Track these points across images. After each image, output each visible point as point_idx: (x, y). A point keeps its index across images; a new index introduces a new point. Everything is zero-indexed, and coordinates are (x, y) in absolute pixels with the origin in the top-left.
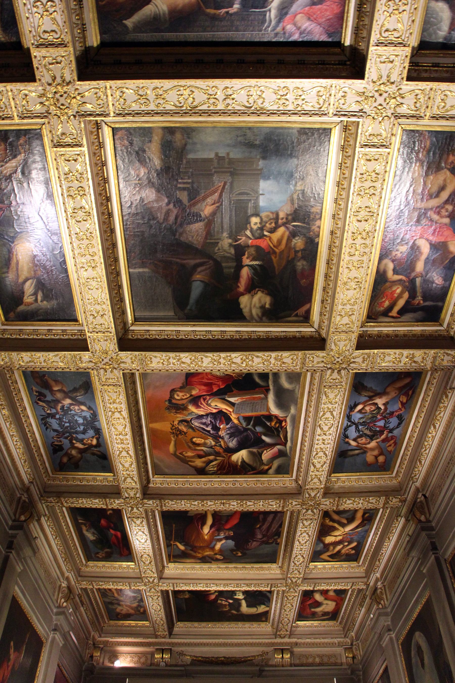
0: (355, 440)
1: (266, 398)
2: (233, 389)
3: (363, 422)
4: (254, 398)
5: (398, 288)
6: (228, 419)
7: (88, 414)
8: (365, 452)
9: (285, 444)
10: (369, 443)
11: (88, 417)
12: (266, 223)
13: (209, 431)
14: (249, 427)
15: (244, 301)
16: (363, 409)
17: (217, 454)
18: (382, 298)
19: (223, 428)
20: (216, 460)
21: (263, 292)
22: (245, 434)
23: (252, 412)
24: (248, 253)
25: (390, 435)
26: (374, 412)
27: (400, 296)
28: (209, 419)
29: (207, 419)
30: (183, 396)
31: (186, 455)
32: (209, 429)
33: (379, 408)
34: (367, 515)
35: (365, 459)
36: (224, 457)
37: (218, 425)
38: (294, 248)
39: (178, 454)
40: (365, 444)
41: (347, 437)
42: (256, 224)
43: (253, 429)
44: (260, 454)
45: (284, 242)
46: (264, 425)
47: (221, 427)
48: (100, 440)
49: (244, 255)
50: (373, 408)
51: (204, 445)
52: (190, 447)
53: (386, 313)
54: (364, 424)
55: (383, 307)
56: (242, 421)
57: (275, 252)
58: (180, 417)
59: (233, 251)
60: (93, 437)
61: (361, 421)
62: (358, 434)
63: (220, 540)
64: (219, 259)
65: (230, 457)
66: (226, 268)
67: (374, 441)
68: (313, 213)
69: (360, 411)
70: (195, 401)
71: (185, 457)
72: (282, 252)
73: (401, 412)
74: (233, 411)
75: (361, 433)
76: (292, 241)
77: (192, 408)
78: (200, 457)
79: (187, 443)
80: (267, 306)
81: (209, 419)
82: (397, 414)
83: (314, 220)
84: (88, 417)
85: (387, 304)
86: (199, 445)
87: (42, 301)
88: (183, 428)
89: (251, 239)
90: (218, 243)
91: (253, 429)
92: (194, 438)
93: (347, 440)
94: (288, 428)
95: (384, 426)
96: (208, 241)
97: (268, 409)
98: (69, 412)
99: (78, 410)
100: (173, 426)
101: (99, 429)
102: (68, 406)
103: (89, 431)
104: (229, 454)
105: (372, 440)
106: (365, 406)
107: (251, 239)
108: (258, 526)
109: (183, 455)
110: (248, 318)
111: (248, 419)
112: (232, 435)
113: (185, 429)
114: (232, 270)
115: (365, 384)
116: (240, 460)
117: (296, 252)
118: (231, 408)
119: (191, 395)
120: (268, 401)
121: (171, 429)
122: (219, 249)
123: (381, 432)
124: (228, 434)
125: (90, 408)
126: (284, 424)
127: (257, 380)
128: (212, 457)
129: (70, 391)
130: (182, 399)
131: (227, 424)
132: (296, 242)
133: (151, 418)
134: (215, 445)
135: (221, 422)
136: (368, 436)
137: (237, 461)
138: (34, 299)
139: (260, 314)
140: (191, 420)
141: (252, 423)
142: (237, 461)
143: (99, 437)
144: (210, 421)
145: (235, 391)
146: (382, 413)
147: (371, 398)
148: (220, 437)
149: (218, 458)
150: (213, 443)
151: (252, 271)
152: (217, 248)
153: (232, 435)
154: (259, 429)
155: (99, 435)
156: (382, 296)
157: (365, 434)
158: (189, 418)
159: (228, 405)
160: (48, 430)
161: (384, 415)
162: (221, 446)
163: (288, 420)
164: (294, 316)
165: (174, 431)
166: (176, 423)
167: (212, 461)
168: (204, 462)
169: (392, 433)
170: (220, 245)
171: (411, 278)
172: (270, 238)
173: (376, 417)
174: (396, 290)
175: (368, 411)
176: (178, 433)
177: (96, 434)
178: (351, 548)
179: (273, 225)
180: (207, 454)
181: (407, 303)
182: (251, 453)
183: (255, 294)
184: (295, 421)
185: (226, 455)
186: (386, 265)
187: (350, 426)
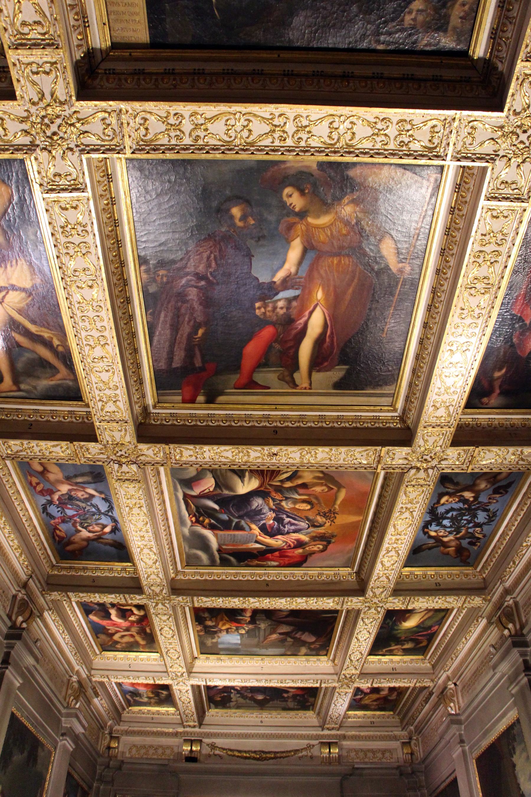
4: (233, 545)
6: (263, 529)
9: (185, 496)
10: (70, 490)
13: (288, 517)
14: (236, 520)
17: (279, 489)
19: (269, 520)
20: (282, 481)
22: (241, 513)
23: (234, 535)
31: (324, 488)
32: (287, 520)
36: (271, 485)
37: (276, 523)
39: (335, 488)
41: (103, 499)
43: (232, 518)
44: (217, 485)
46: (218, 520)
48: (436, 501)
51: (295, 501)
52: (317, 498)
56: (245, 526)
58: (321, 530)
63: (286, 283)
65: (261, 486)
70: (300, 544)
71: (326, 485)
74: (257, 536)
77: (304, 538)
78: (304, 486)
79: (319, 503)
81: (286, 529)
86: (304, 501)
88: (320, 519)
91: (232, 518)
93: (103, 496)
94: (187, 515)
97: (216, 536)
104: (262, 489)
105: (67, 494)
108: (200, 332)
109: (328, 487)
111: (239, 528)
112: (258, 512)
116: (246, 479)
120: (218, 542)
121: (336, 518)
124: (264, 514)
127: (232, 559)
128: (288, 485)
131: (264, 524)
133: (357, 527)
134: (281, 501)
135: (272, 527)
137: (250, 478)
140: (309, 527)
141: (234, 524)
142: (250, 478)
144: (285, 527)
145: (255, 552)
148: (274, 511)
149: (279, 484)
150: (284, 503)
153: (258, 512)
154: (225, 517)
158: (311, 529)
159: (263, 542)
162: (274, 500)
163: (189, 523)
165: (333, 515)
166: (328, 524)
167: (289, 479)
168: (300, 477)
176: (327, 514)
180: (294, 489)
182: (230, 488)
184: (181, 521)
185: (266, 488)
187: (108, 511)
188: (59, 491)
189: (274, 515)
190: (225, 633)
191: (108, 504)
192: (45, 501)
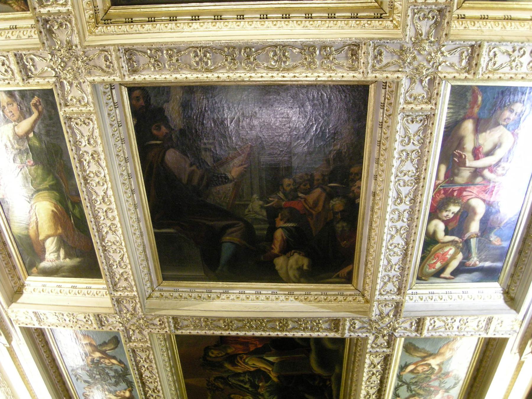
1: (308, 357)
2: (272, 348)
3: (416, 382)
5: (451, 249)
6: (267, 378)
7: (119, 368)
11: (120, 370)
12: (300, 184)
13: (247, 389)
15: (280, 262)
16: (415, 369)
18: (433, 260)
21: (299, 254)
24: (282, 215)
26: (427, 373)
27: (453, 257)
28: (247, 377)
29: (244, 377)
30: (218, 354)
32: (247, 386)
33: (433, 369)
37: (256, 383)
38: (333, 209)
42: (289, 185)
45: (321, 203)
48: (133, 392)
49: (277, 217)
50: (426, 368)
53: (438, 274)
55: (434, 268)
57: (311, 214)
58: (216, 374)
59: (265, 214)
60: (126, 390)
61: (414, 381)
64: (250, 221)
66: (257, 229)
68: (352, 174)
69: (412, 371)
72: (319, 213)
74: (272, 370)
75: (414, 392)
76: (329, 203)
77: (228, 366)
80: (305, 267)
81: (247, 377)
83: (354, 181)
84: (120, 370)
85: (438, 265)
87: (65, 258)
89: (283, 200)
90: (248, 205)
92: (232, 394)
96: (237, 203)
97: (311, 368)
98: (100, 365)
99: (109, 363)
100: (209, 382)
101: (132, 382)
102: (98, 359)
103: (121, 384)
106: (417, 367)
107: (283, 200)
110: (284, 279)
113: (221, 386)
114: (265, 232)
115: (417, 345)
117: (335, 213)
118: (270, 367)
119: (227, 354)
121: (207, 385)
122: (249, 211)
125: (120, 362)
126: (328, 383)
129: (100, 345)
130: (216, 357)
131: (267, 382)
132: (334, 203)
138: (56, 256)
139: (297, 276)
140: (228, 378)
143: (132, 390)
144: (248, 379)
146: (438, 373)
147: (423, 358)
151: (287, 232)
152: (247, 210)
155: (132, 387)
156: (433, 257)
158: (225, 375)
160: (79, 381)
161: (439, 375)
163: (333, 379)
164: (335, 278)
166: (212, 379)
169: (448, 392)
170: (250, 206)
171: (465, 238)
172: (305, 200)
174: (448, 251)
175: (421, 371)
177: (128, 387)
179: (308, 186)
181: (462, 264)
183: (291, 256)
186: (436, 226)
187: (401, 386)
189: (259, 390)
190: (317, 176)
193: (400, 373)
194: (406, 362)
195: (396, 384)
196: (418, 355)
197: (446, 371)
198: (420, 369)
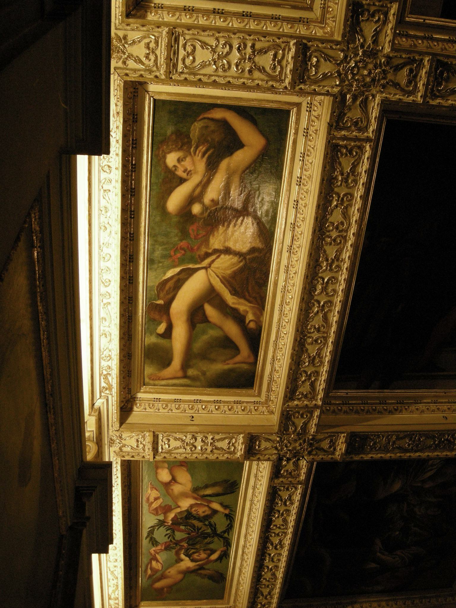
0: (215, 512)
3: (206, 538)
8: (195, 490)
10: (192, 506)
25: (161, 517)
26: (193, 551)
33: (187, 555)
34: (162, 328)
35: (192, 475)
40: (196, 504)
47: (397, 533)
50: (196, 556)
54: (205, 536)
61: (208, 540)
62: (212, 521)
67: (184, 509)
69: (213, 552)
73: (154, 549)
75: (207, 523)
82: (159, 547)
93: (227, 512)
95: (174, 532)
105: (187, 511)
106: (208, 558)
123: (175, 521)
136: (195, 518)
146: (181, 549)
147: (201, 568)
157: (201, 521)
161: (178, 547)
173: (189, 545)
175: (201, 552)
178: (182, 181)
187: (224, 532)
188: (179, 507)
191: (229, 522)
192: (156, 521)
193: (228, 549)
194: (221, 562)
195: (230, 533)
196: (208, 571)
197: (169, 552)
198: (203, 556)
